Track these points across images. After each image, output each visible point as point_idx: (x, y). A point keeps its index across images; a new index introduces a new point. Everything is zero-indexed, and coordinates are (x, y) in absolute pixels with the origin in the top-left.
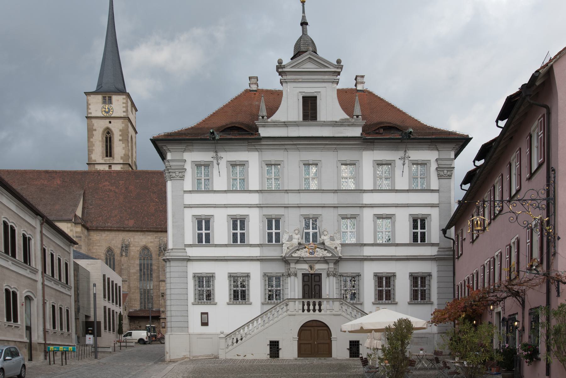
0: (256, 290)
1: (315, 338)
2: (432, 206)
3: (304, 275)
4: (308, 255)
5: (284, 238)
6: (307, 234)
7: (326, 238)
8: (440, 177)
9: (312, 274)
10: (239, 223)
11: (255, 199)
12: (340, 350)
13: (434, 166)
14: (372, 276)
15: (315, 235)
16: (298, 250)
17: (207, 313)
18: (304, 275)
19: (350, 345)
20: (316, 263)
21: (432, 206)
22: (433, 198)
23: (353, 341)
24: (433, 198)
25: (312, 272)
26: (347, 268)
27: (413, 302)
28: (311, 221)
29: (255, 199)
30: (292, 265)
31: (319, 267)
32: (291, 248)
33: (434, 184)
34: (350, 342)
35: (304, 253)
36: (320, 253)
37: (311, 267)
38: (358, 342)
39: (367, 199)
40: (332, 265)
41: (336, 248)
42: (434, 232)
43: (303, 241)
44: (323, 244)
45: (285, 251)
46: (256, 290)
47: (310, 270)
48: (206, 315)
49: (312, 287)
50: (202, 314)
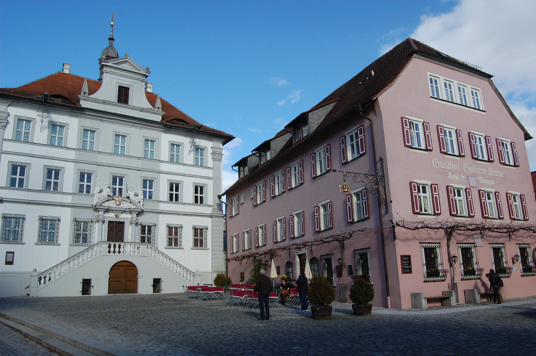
0: (65, 232)
1: (123, 276)
2: (209, 178)
3: (110, 222)
4: (114, 205)
5: (95, 190)
6: (115, 190)
7: (131, 194)
8: (214, 159)
9: (116, 222)
10: (53, 174)
11: (71, 155)
12: (145, 287)
13: (210, 151)
14: (165, 226)
15: (120, 190)
16: (107, 201)
17: (13, 253)
18: (110, 222)
19: (154, 282)
20: (122, 213)
21: (209, 178)
22: (210, 173)
23: (156, 279)
24: (210, 173)
25: (117, 220)
26: (145, 219)
27: (195, 248)
28: (118, 180)
29: (71, 155)
30: (101, 213)
31: (123, 217)
32: (102, 199)
33: (210, 162)
34: (154, 279)
35: (111, 204)
36: (126, 205)
37: (117, 216)
38: (160, 279)
39: (164, 167)
40: (135, 215)
41: (139, 202)
42: (210, 197)
43: (111, 194)
44: (128, 198)
45: (95, 201)
46: (65, 232)
47: (115, 218)
48: (12, 254)
49: (116, 232)
50: (7, 253)
